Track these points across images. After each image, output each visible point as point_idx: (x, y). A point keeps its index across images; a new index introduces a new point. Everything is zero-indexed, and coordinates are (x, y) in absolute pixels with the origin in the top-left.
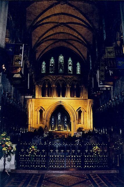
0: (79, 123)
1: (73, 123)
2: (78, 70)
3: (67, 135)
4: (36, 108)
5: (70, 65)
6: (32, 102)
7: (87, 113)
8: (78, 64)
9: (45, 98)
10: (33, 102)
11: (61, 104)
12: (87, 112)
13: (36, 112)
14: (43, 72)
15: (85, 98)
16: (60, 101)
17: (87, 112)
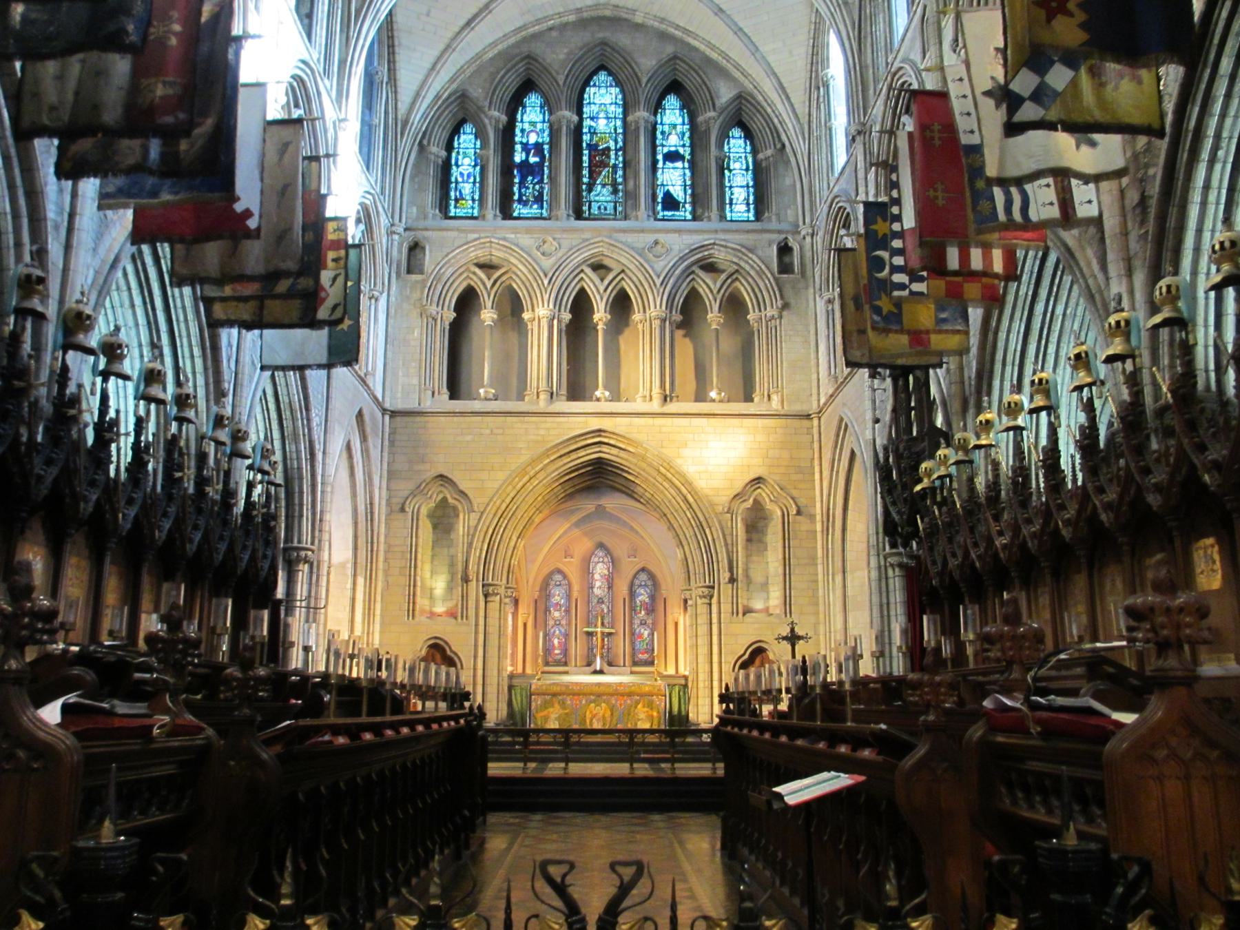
0: (747, 611)
1: (702, 609)
2: (739, 195)
3: (650, 705)
4: (404, 487)
5: (672, 157)
6: (364, 438)
7: (819, 527)
8: (737, 145)
9: (477, 405)
10: (374, 445)
11: (608, 454)
12: (812, 517)
13: (402, 524)
14: (460, 213)
15: (797, 408)
16: (599, 432)
17: (818, 518)
